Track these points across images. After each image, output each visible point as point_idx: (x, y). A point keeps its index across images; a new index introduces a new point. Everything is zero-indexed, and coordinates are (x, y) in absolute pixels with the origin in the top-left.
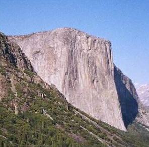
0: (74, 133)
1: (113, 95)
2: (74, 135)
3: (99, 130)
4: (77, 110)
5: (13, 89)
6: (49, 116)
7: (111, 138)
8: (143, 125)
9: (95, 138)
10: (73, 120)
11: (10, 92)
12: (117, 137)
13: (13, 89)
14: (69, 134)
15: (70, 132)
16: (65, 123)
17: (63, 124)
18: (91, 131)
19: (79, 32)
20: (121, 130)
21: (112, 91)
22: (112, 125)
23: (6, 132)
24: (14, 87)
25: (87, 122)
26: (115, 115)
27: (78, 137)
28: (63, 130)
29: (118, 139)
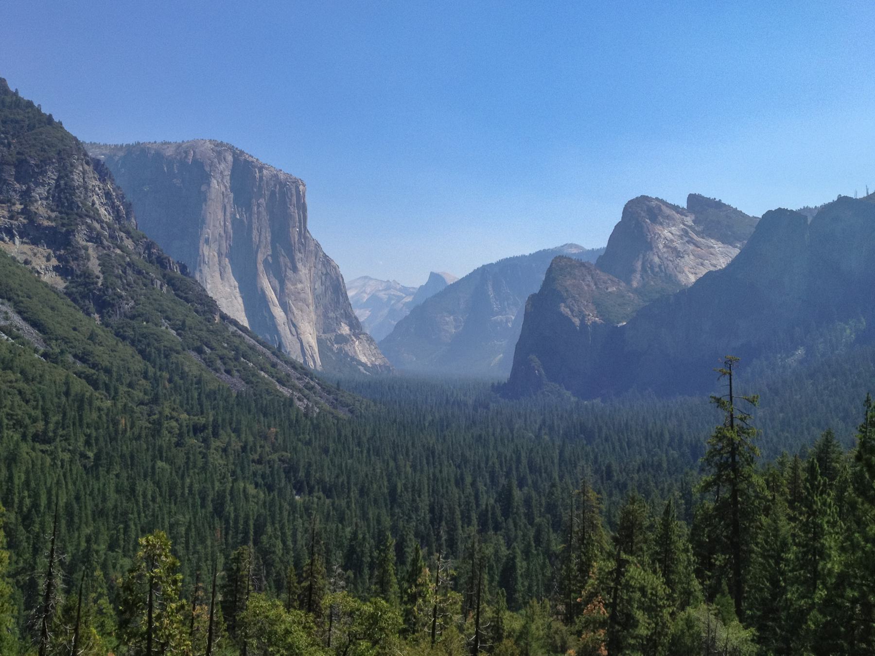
0: (228, 372)
1: (302, 295)
2: (224, 376)
3: (274, 365)
4: (235, 323)
5: (94, 265)
6: (174, 332)
7: (299, 384)
8: (353, 359)
9: (266, 384)
10: (226, 345)
11: (87, 275)
12: (312, 383)
13: (94, 265)
14: (218, 375)
15: (217, 370)
16: (208, 351)
17: (205, 353)
18: (262, 370)
19: (242, 152)
20: (312, 367)
21: (299, 286)
22: (294, 357)
23: (79, 365)
24: (98, 262)
25: (252, 348)
26: (302, 337)
27: (234, 380)
28: (204, 366)
29: (313, 387)
